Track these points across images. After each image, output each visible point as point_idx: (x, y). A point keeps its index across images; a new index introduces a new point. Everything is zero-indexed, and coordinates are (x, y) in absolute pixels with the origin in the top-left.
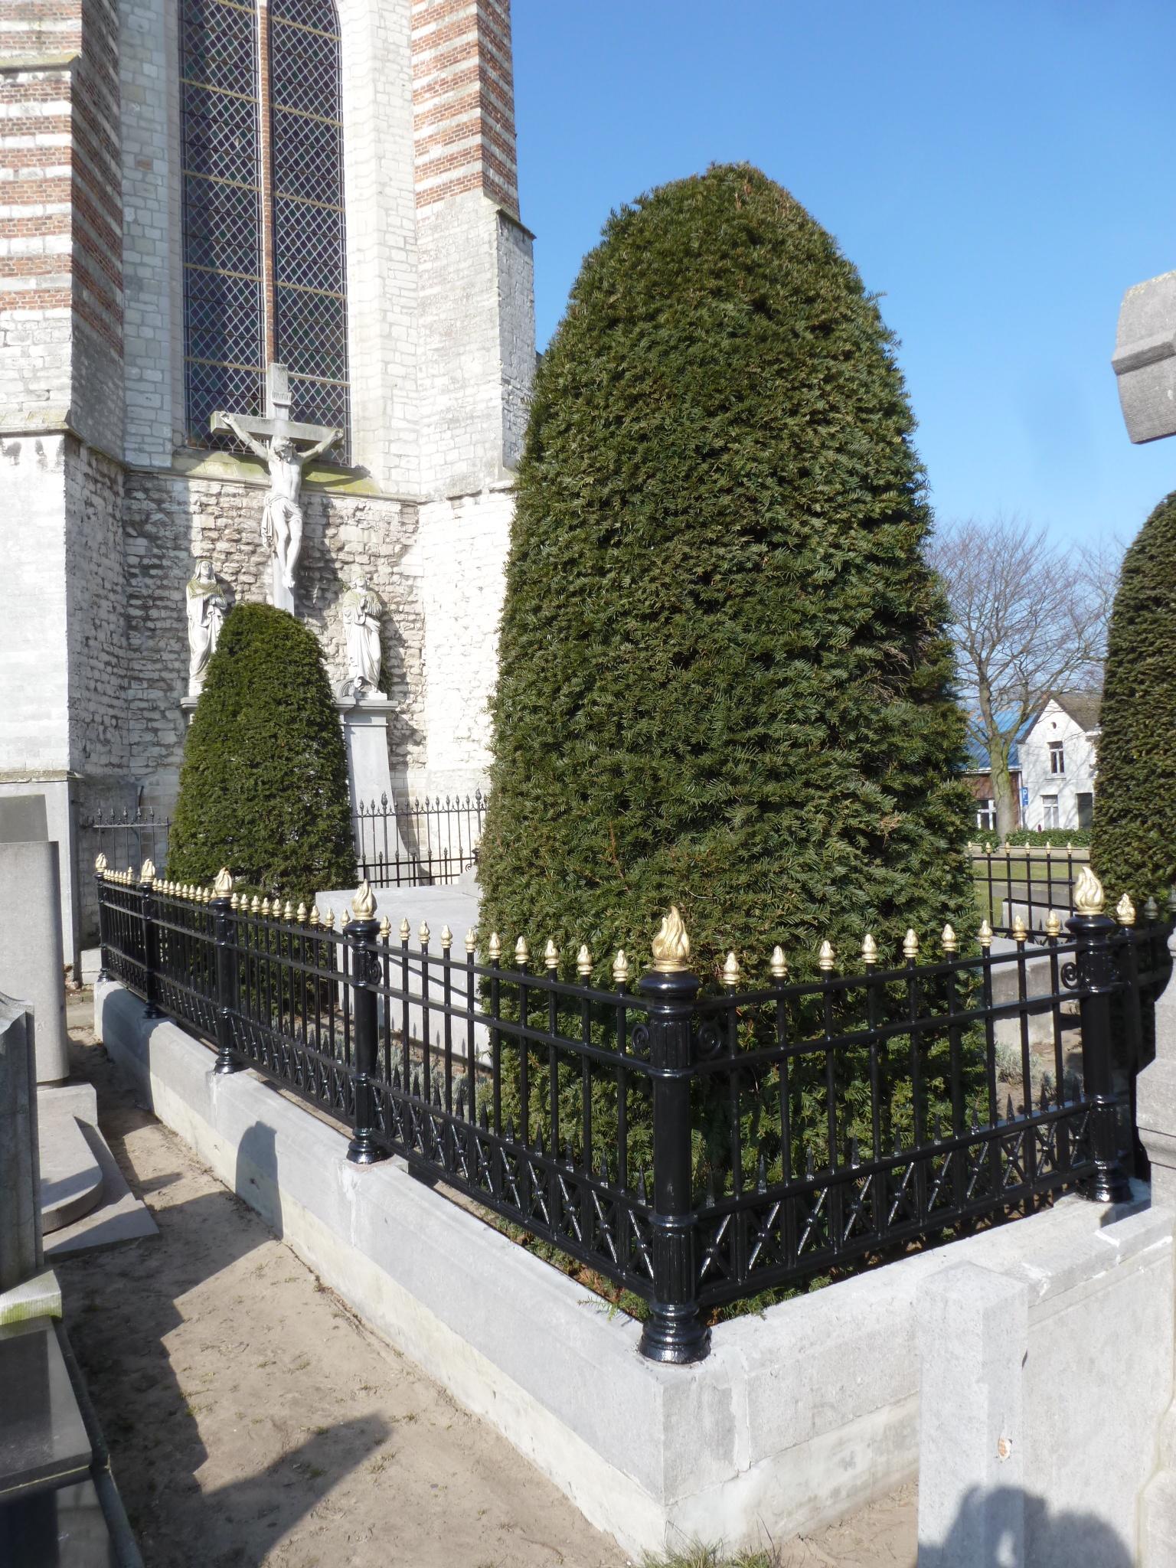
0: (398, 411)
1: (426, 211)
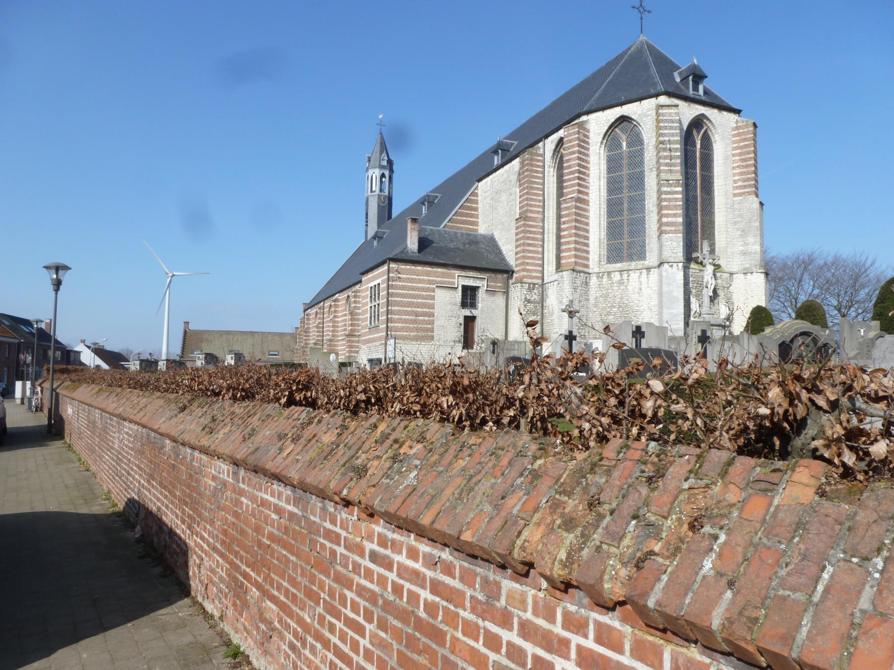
0: (729, 250)
1: (735, 199)
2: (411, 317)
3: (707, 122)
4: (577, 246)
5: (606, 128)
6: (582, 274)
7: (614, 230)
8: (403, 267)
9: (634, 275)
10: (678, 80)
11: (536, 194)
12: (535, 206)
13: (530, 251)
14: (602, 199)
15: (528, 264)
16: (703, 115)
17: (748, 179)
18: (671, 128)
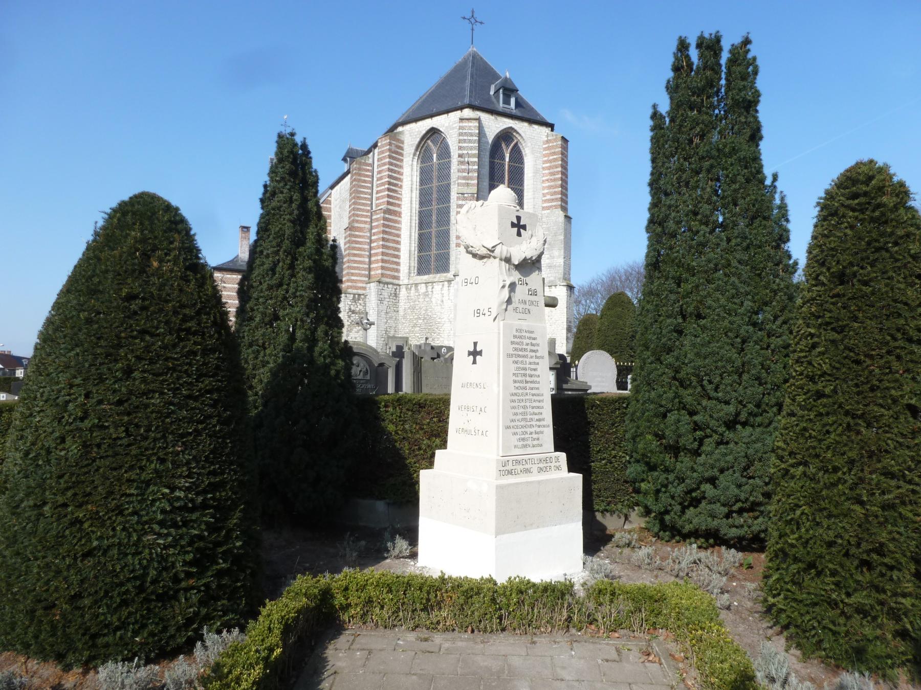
3: (517, 136)
4: (385, 258)
5: (418, 140)
6: (390, 286)
7: (423, 242)
9: (437, 287)
10: (492, 93)
11: (364, 204)
12: (362, 216)
13: (355, 262)
14: (414, 211)
15: (353, 274)
16: (511, 128)
17: (555, 193)
18: (470, 141)
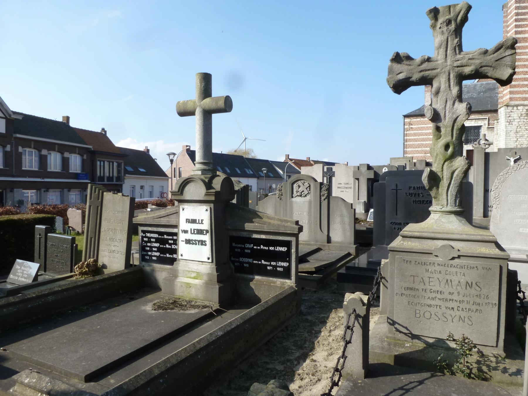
2: (421, 155)
6: (519, 108)
8: (414, 120)
